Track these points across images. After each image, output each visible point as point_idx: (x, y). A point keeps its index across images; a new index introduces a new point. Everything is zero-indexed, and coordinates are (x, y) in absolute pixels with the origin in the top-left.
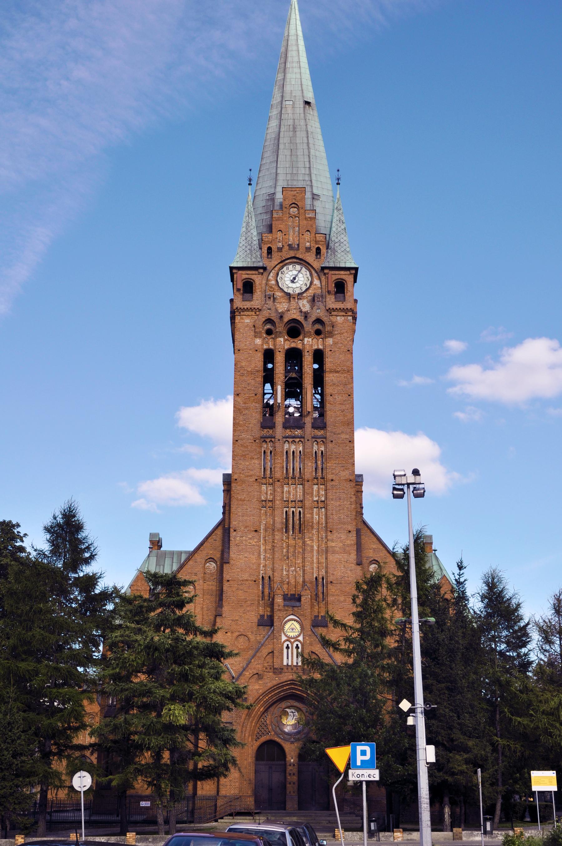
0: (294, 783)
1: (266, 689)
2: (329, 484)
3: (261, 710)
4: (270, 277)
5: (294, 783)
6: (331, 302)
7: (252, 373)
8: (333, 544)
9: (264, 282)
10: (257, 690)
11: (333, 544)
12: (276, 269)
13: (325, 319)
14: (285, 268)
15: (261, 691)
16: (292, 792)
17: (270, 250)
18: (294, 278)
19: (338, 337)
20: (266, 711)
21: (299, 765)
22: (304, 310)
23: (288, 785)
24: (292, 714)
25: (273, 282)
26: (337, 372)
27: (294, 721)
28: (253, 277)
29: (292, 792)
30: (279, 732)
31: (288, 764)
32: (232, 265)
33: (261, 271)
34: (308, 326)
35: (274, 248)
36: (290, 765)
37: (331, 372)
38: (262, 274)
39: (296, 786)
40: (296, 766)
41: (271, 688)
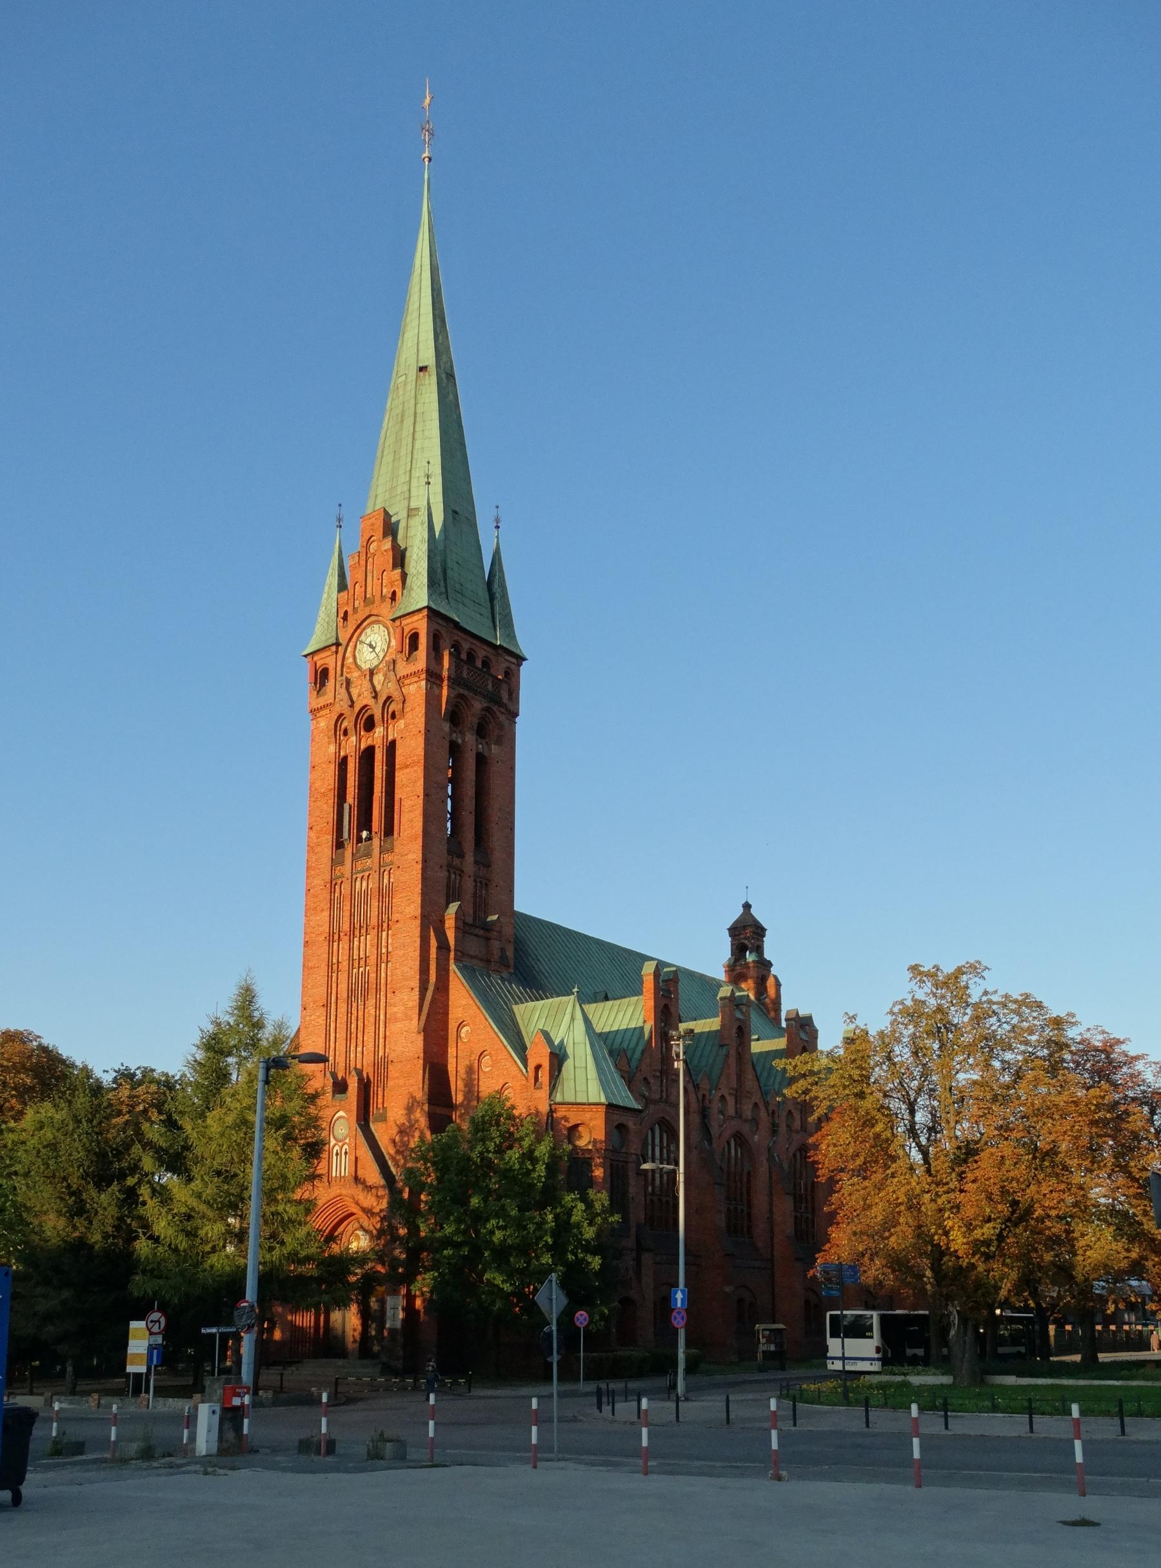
2: (394, 927)
4: (348, 654)
6: (403, 669)
7: (324, 795)
8: (395, 1010)
9: (339, 663)
11: (395, 1010)
12: (354, 639)
13: (396, 694)
14: (363, 638)
17: (346, 612)
18: (370, 646)
19: (409, 716)
22: (378, 688)
25: (351, 660)
26: (407, 767)
28: (327, 661)
32: (305, 653)
33: (334, 648)
34: (377, 713)
35: (350, 612)
37: (401, 768)
38: (337, 652)
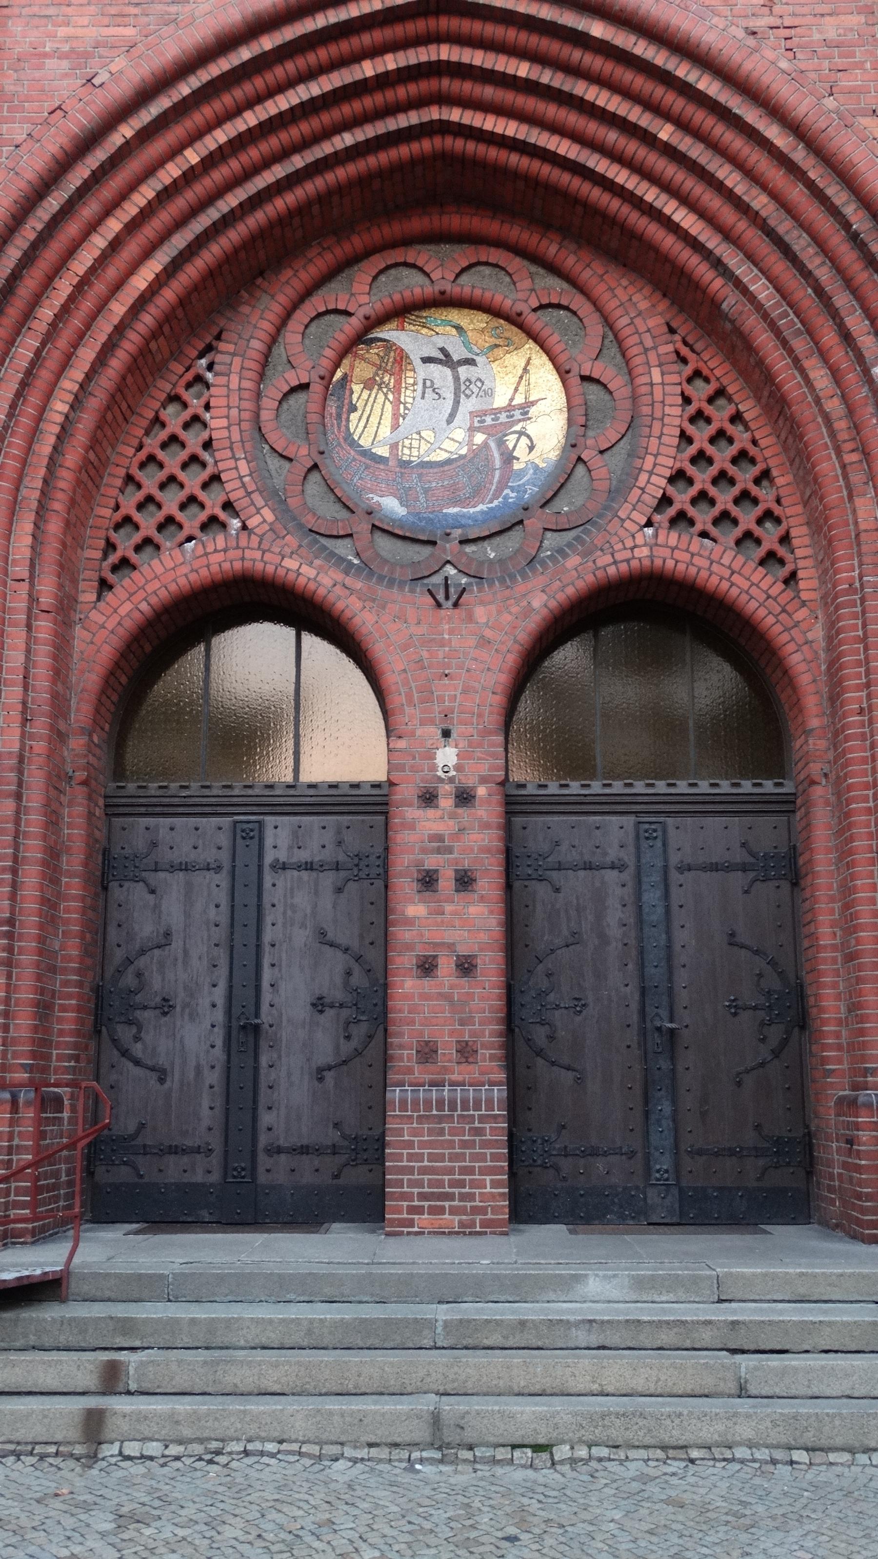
0: (466, 967)
1: (172, 47)
3: (141, 281)
5: (466, 967)
10: (78, 57)
15: (119, 63)
16: (447, 1052)
20: (195, 320)
21: (515, 805)
23: (407, 987)
24: (441, 374)
27: (460, 434)
29: (447, 1052)
30: (329, 510)
31: (407, 791)
36: (429, 798)
39: (485, 994)
40: (487, 809)
41: (226, 43)
